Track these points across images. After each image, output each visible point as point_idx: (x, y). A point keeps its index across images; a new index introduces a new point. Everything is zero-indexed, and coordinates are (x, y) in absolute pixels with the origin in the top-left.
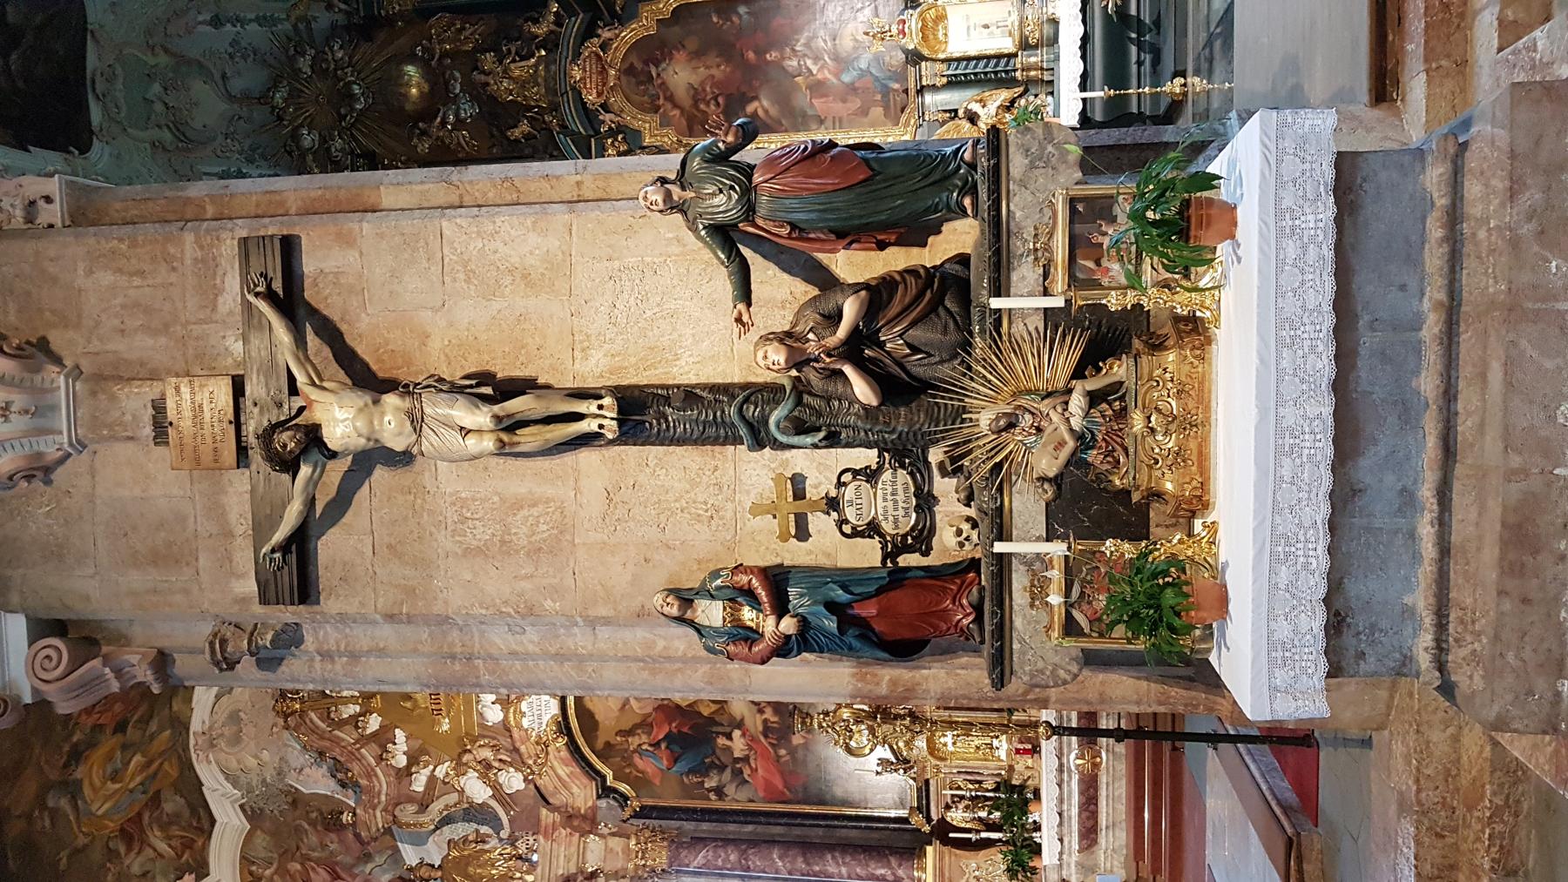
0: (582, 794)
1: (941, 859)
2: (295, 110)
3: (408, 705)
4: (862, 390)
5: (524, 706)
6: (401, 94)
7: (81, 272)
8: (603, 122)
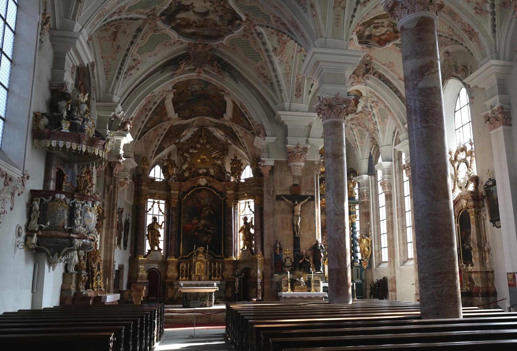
0: (184, 189)
1: (176, 262)
3: (203, 154)
4: (301, 261)
5: (204, 179)
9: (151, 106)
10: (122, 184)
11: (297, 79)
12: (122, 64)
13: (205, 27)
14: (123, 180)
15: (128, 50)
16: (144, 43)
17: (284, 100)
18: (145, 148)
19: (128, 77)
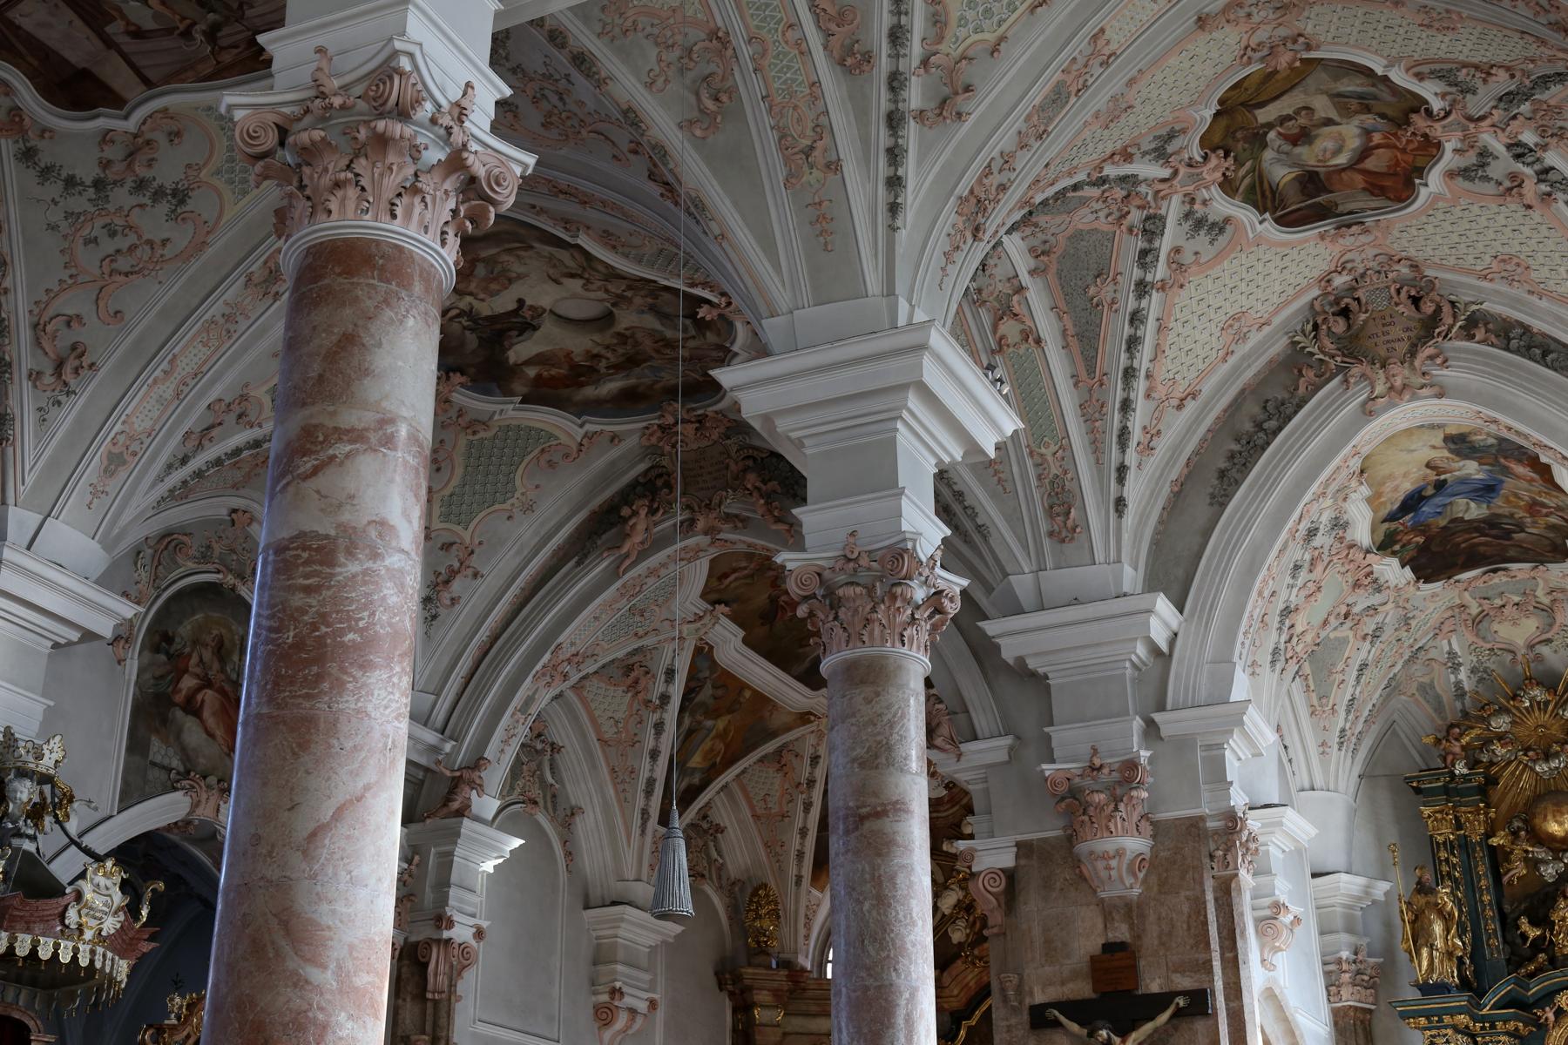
2: (1526, 708)
6: (1545, 817)
7: (1188, 893)
8: (1544, 1010)
9: (660, 687)
10: (604, 1016)
11: (1037, 465)
13: (645, 361)
14: (605, 998)
16: (455, 481)
17: (1009, 570)
18: (767, 846)
19: (442, 611)
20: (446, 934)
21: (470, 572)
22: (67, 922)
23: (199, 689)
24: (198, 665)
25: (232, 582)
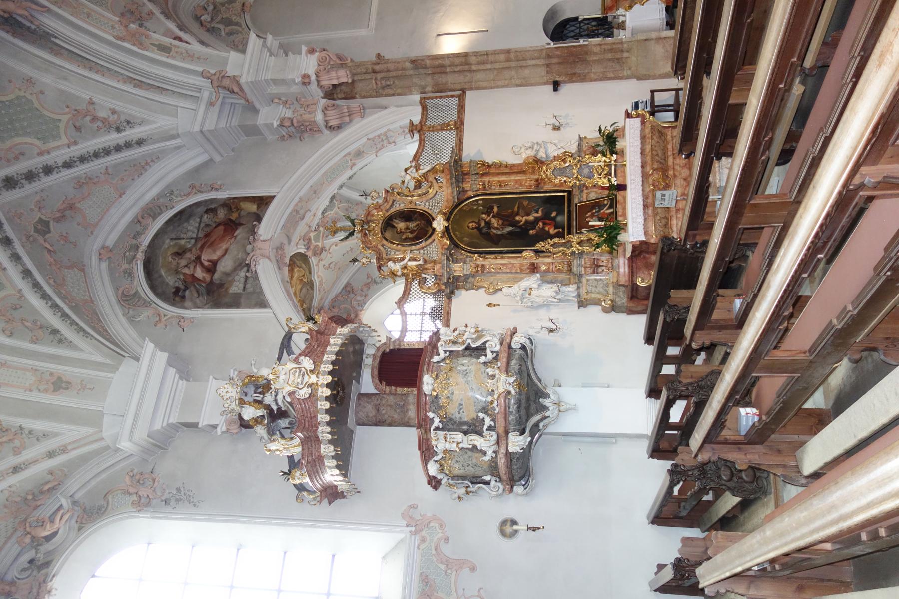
12: (107, 152)
15: (68, 165)
16: (29, 140)
19: (123, 118)
20: (313, 78)
21: (91, 108)
22: (307, 396)
23: (202, 264)
24: (189, 268)
25: (141, 254)
